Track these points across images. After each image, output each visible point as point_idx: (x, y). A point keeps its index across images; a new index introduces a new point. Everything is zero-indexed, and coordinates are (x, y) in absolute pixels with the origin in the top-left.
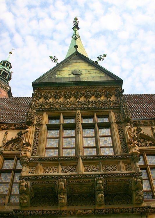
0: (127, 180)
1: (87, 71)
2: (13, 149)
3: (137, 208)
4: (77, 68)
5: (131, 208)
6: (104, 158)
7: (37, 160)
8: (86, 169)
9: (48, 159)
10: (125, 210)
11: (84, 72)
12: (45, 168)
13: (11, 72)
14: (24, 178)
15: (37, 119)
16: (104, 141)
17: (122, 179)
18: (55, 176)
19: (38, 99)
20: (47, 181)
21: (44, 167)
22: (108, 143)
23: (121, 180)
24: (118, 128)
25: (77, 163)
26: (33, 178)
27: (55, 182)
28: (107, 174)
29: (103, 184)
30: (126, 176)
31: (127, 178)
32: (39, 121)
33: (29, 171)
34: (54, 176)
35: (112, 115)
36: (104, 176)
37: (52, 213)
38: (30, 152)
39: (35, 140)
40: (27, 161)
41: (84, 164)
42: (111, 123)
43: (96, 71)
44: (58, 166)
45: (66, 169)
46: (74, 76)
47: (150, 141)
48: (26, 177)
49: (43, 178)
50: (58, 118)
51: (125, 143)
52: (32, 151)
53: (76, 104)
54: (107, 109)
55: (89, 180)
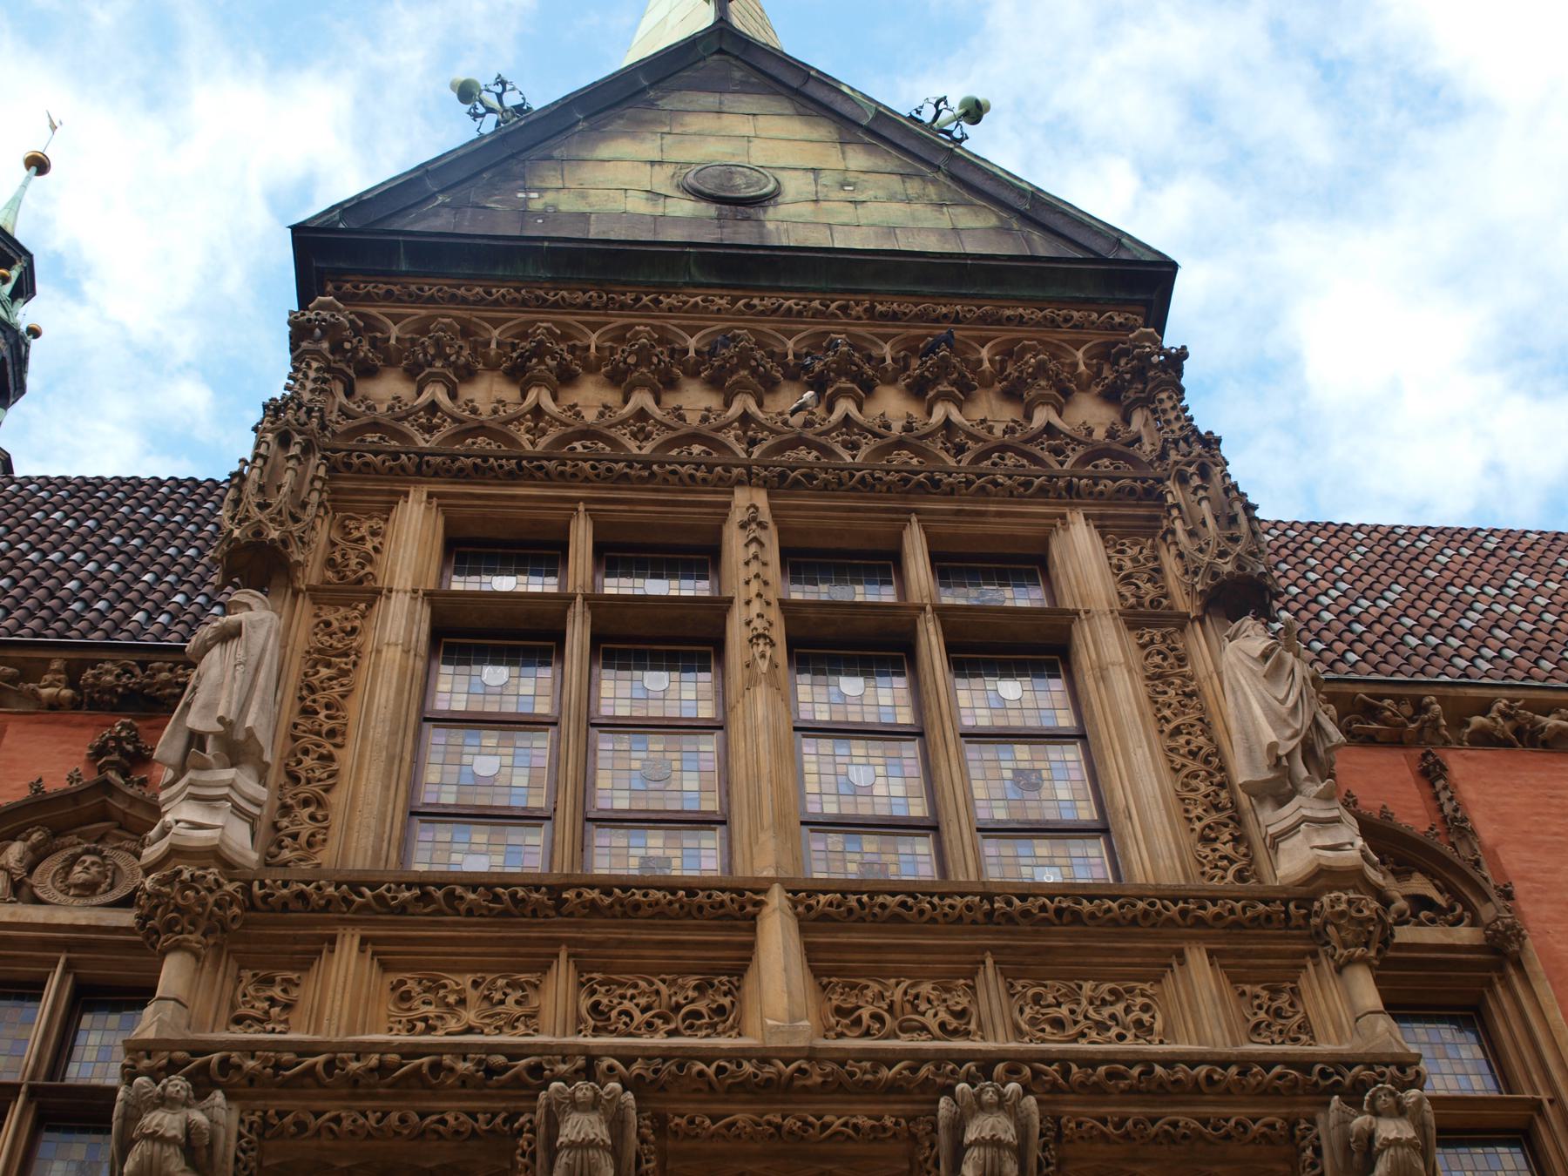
0: (1272, 1126)
1: (826, 179)
2: (38, 891)
6: (1026, 913)
7: (329, 902)
8: (839, 1011)
11: (795, 185)
12: (411, 984)
13: (23, 328)
14: (172, 1067)
15: (333, 544)
16: (1008, 774)
19: (351, 372)
21: (394, 978)
22: (1045, 794)
24: (1144, 668)
25: (751, 946)
26: (278, 1066)
27: (513, 1117)
28: (1064, 1061)
30: (1267, 1093)
31: (1274, 1115)
32: (353, 561)
33: (233, 1007)
35: (1081, 551)
36: (1036, 1074)
38: (252, 820)
39: (306, 724)
40: (218, 904)
41: (824, 966)
42: (1077, 613)
43: (914, 187)
44: (545, 968)
45: (627, 1005)
46: (711, 210)
47: (1417, 875)
48: (195, 1053)
50: (545, 552)
51: (1223, 794)
52: (275, 827)
53: (720, 436)
54: (1024, 490)
55: (876, 1108)
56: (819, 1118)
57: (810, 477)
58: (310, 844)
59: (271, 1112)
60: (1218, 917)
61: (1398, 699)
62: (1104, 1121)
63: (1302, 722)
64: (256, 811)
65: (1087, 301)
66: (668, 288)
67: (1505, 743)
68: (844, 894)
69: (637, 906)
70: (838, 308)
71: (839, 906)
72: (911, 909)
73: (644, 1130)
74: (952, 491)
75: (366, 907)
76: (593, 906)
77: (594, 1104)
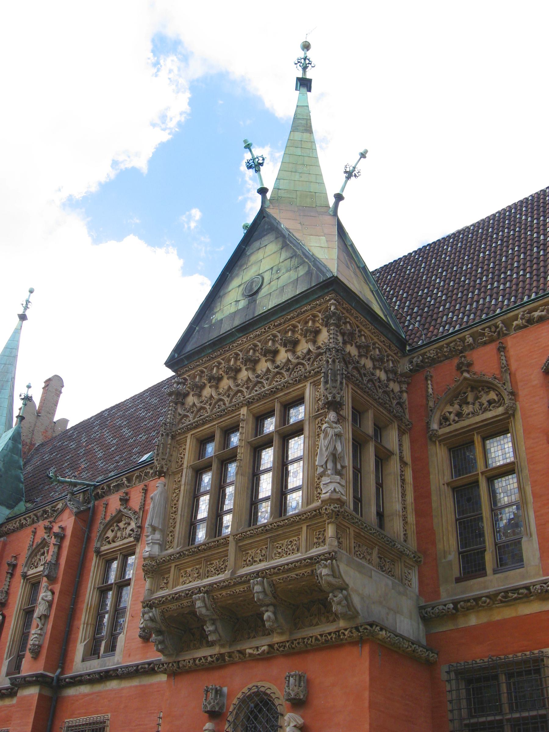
3: (346, 630)
4: (256, 271)
5: (335, 633)
10: (324, 638)
11: (267, 277)
18: (189, 590)
20: (181, 602)
23: (297, 575)
29: (264, 592)
31: (309, 570)
34: (187, 592)
40: (151, 568)
45: (212, 569)
49: (176, 598)
54: (297, 381)
57: (254, 399)
58: (171, 543)
60: (306, 517)
61: (489, 327)
63: (331, 448)
64: (158, 542)
65: (319, 297)
66: (233, 342)
67: (525, 327)
69: (211, 547)
70: (268, 328)
74: (282, 390)
75: (173, 560)
76: (204, 549)
77: (199, 599)
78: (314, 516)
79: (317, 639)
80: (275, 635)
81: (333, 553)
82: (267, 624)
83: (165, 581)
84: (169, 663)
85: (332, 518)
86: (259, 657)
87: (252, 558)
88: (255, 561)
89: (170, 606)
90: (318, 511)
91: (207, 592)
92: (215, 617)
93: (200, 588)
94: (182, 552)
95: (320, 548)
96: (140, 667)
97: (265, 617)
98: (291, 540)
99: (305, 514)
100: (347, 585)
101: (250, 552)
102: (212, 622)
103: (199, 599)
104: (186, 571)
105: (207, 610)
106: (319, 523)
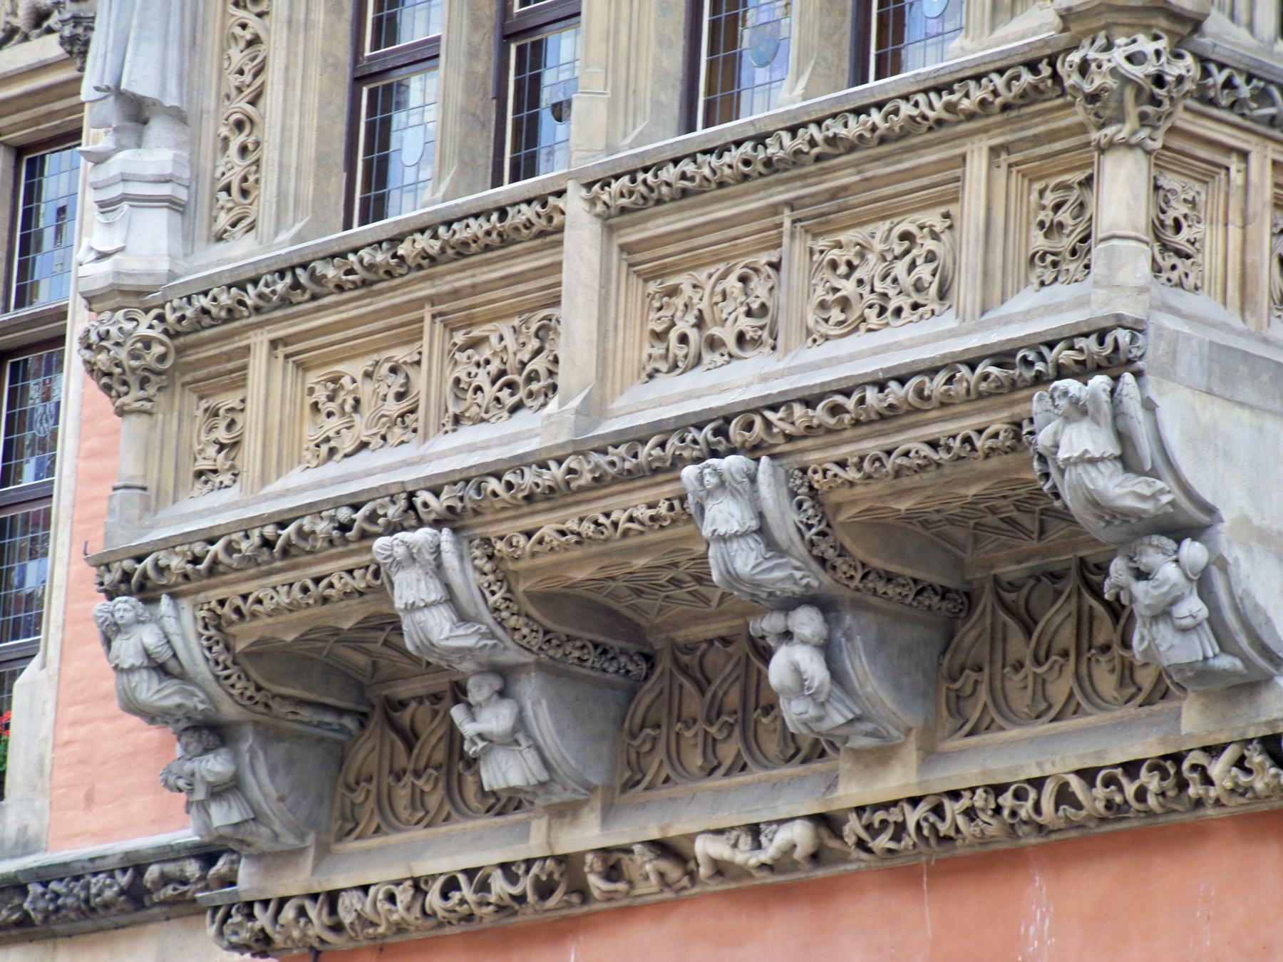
3: (1213, 751)
5: (1157, 766)
7: (230, 311)
9: (303, 276)
10: (1100, 791)
17: (951, 427)
23: (934, 445)
31: (997, 421)
34: (344, 514)
37: (492, 898)
38: (172, 204)
40: (134, 356)
41: (648, 267)
45: (482, 379)
49: (279, 544)
55: (650, 494)
56: (607, 515)
59: (214, 604)
60: (983, 102)
62: (842, 464)
64: (165, 190)
68: (633, 174)
69: (465, 244)
71: (631, 193)
72: (692, 179)
73: (477, 562)
75: (257, 310)
76: (425, 255)
78: (1029, 96)
79: (1064, 796)
80: (843, 763)
81: (1123, 336)
82: (794, 711)
83: (222, 435)
84: (282, 901)
85: (1121, 119)
86: (771, 879)
87: (700, 323)
88: (714, 344)
89: (257, 588)
90: (1046, 71)
91: (450, 519)
92: (512, 655)
93: (412, 495)
94: (304, 266)
95: (1061, 292)
96: (153, 872)
97: (778, 671)
98: (906, 226)
99: (978, 78)
100: (1210, 510)
101: (684, 281)
102: (497, 683)
103: (413, 557)
104: (335, 380)
105: (463, 617)
106: (1053, 136)
